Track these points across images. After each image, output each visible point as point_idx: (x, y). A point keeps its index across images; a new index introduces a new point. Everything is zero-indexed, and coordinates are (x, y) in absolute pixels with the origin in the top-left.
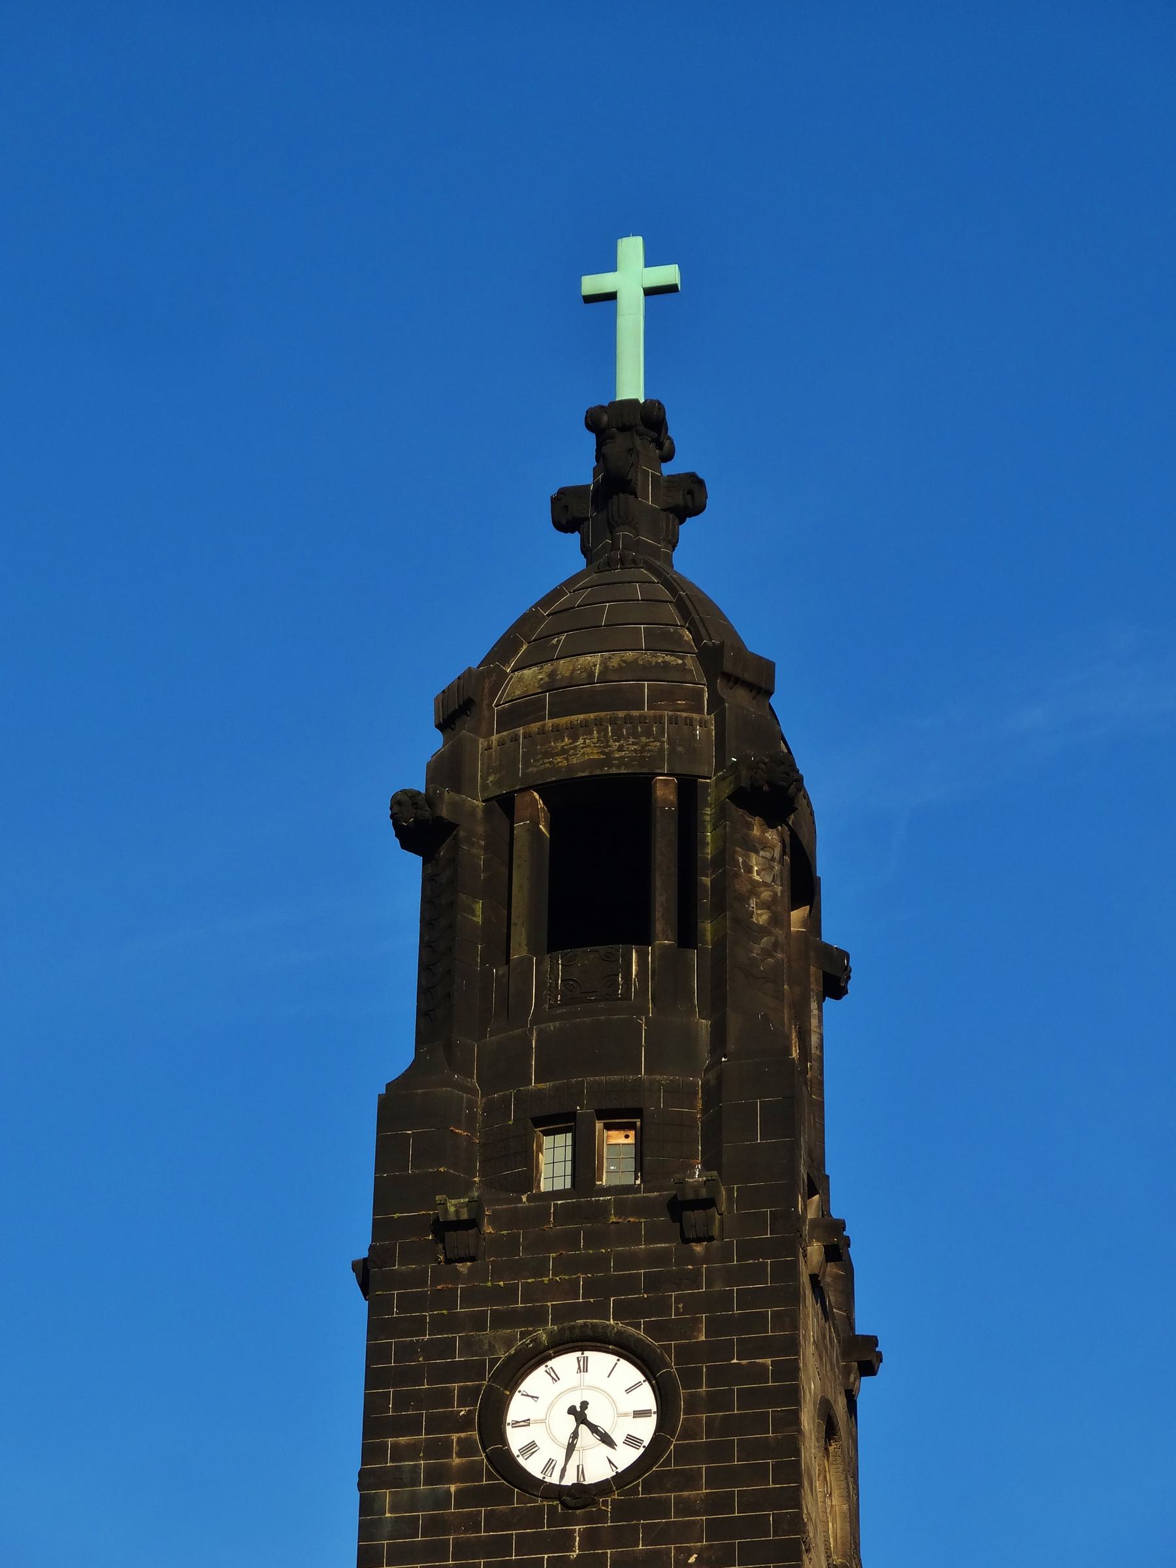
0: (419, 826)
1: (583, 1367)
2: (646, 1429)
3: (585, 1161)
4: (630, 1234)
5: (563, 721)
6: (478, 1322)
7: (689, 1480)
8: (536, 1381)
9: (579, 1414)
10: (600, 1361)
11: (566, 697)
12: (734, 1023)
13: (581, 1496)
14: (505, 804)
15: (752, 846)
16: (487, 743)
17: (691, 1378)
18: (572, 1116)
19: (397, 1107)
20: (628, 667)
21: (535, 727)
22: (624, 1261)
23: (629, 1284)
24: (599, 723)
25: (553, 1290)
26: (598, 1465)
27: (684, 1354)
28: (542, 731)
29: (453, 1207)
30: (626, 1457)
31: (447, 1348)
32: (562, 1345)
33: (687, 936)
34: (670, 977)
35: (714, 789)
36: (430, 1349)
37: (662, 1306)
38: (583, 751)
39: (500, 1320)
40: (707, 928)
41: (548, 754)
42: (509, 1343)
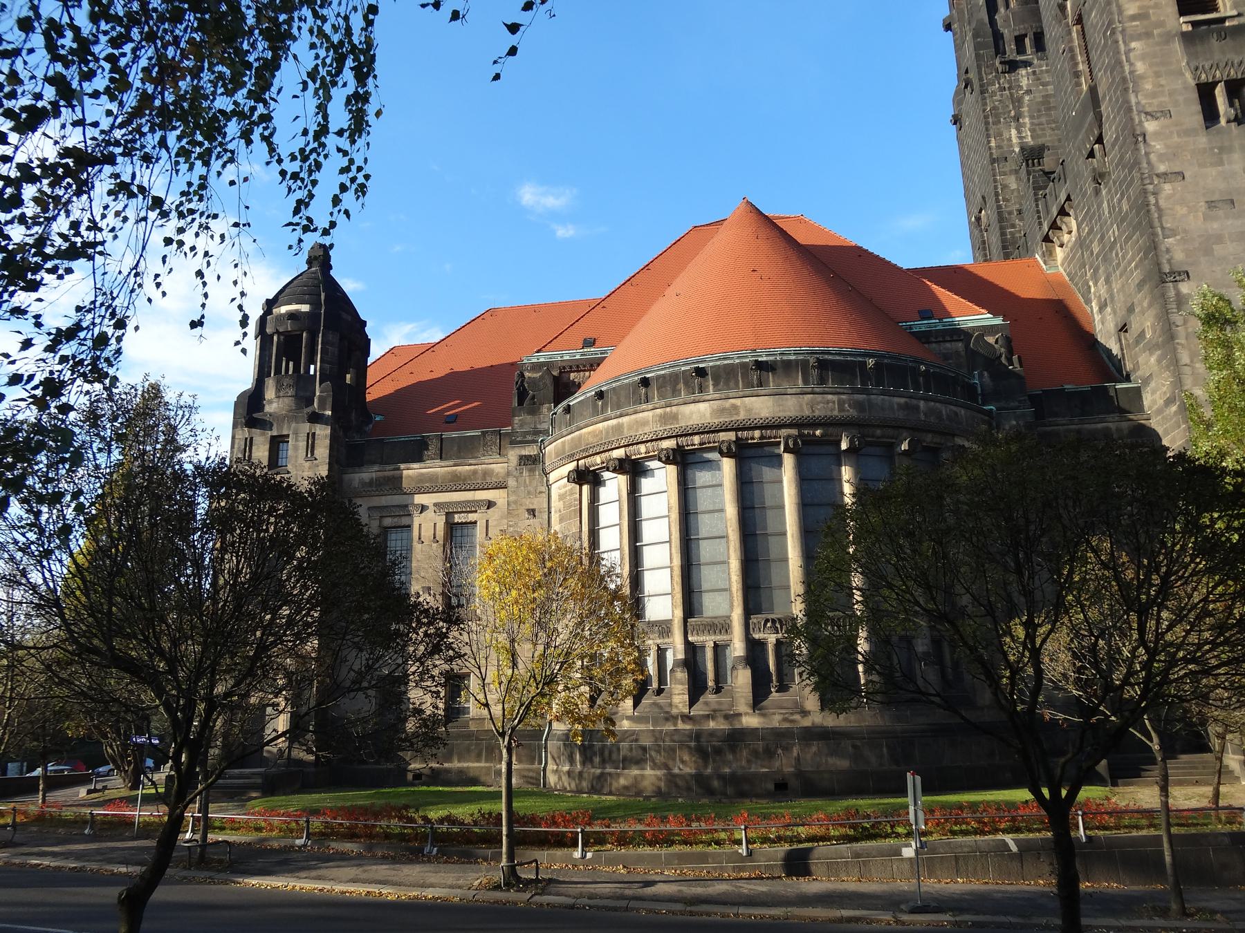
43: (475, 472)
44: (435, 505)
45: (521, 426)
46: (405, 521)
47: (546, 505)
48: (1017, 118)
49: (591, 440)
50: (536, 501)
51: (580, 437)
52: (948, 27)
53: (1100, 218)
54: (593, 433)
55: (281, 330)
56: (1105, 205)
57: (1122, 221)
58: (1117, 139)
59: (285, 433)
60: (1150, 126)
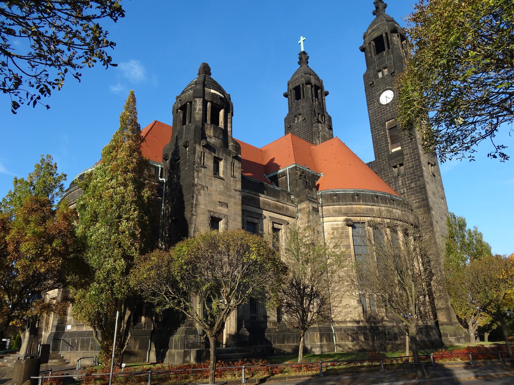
0: (363, 49)
6: (375, 92)
11: (373, 31)
12: (394, 54)
13: (387, 105)
14: (370, 43)
15: (394, 36)
16: (367, 39)
19: (364, 76)
26: (389, 101)
29: (371, 83)
30: (391, 99)
32: (383, 91)
33: (389, 48)
34: (388, 53)
35: (389, 32)
38: (376, 35)
40: (391, 46)
43: (283, 207)
44: (270, 217)
45: (308, 193)
46: (256, 221)
47: (322, 230)
48: (319, 137)
49: (359, 210)
50: (319, 227)
51: (352, 208)
52: (286, 95)
53: (395, 184)
54: (360, 208)
55: (214, 102)
56: (400, 182)
57: (410, 189)
58: (412, 167)
59: (221, 157)
60: (424, 168)
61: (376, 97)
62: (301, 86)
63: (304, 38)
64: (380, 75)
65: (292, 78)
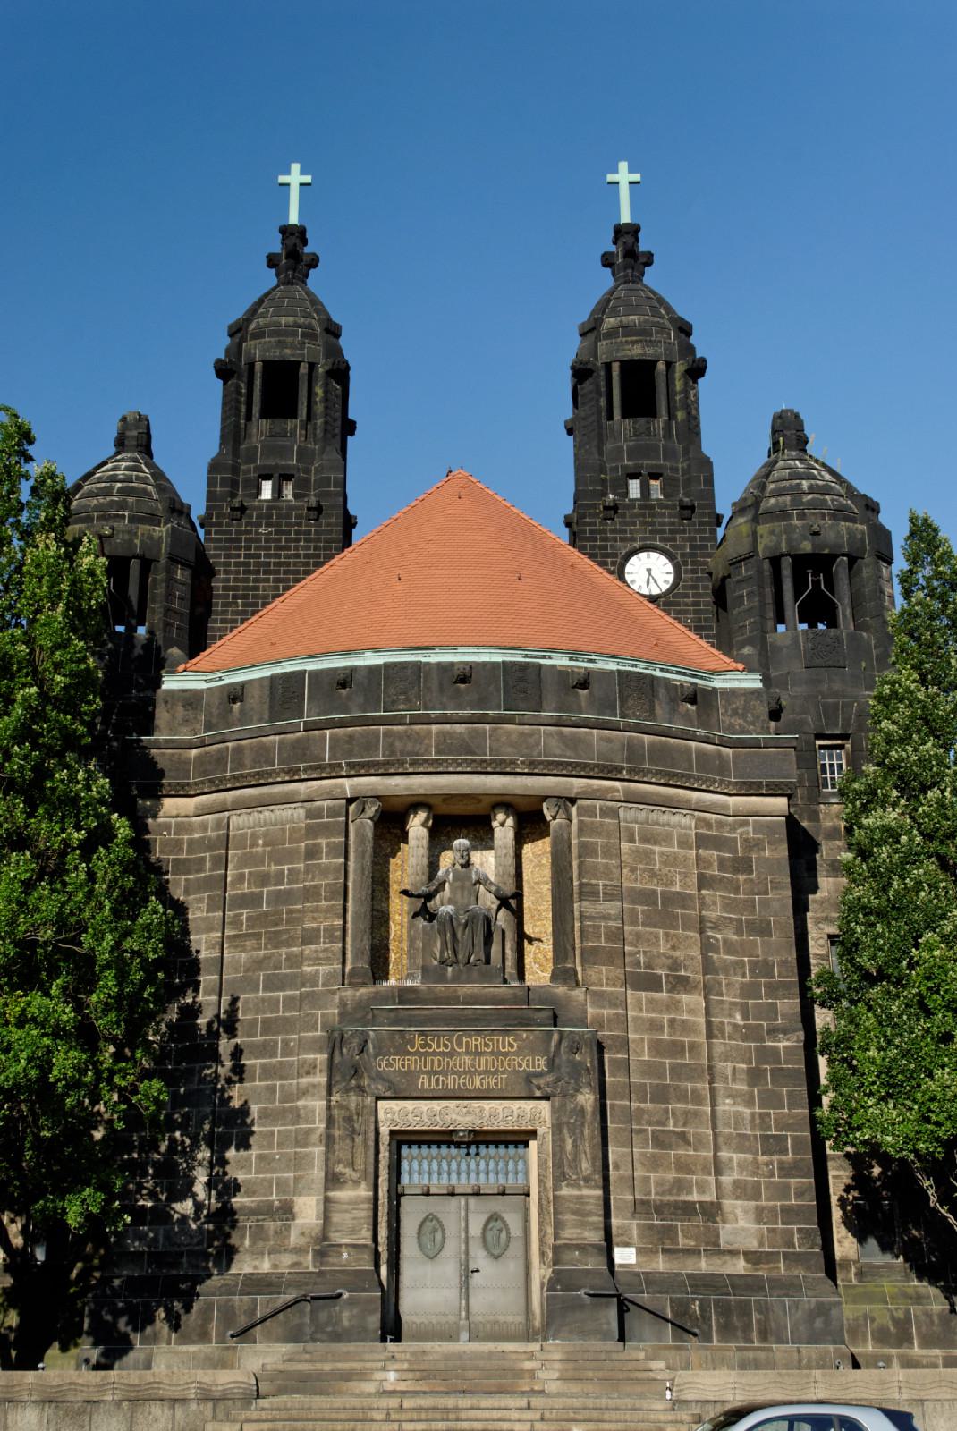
1: (649, 557)
2: (671, 578)
3: (645, 489)
4: (663, 515)
5: (624, 339)
7: (687, 596)
8: (633, 560)
9: (649, 570)
10: (654, 555)
11: (627, 329)
17: (685, 563)
18: (640, 474)
20: (646, 321)
21: (619, 340)
22: (663, 524)
23: (663, 531)
24: (641, 341)
25: (637, 531)
27: (683, 555)
28: (621, 342)
30: (665, 587)
31: (605, 547)
33: (671, 415)
36: (601, 547)
37: (675, 540)
38: (636, 352)
39: (622, 540)
41: (624, 350)
42: (626, 547)
61: (615, 555)
62: (303, 369)
63: (308, 179)
64: (634, 488)
65: (253, 312)
